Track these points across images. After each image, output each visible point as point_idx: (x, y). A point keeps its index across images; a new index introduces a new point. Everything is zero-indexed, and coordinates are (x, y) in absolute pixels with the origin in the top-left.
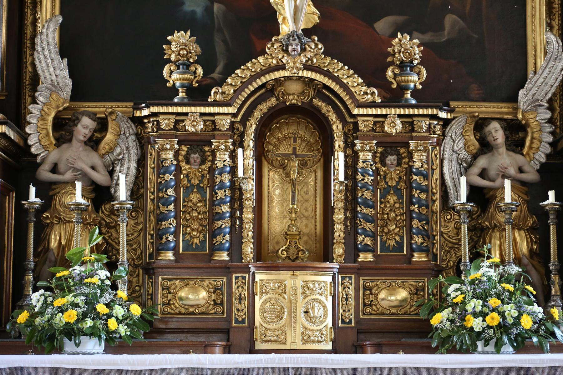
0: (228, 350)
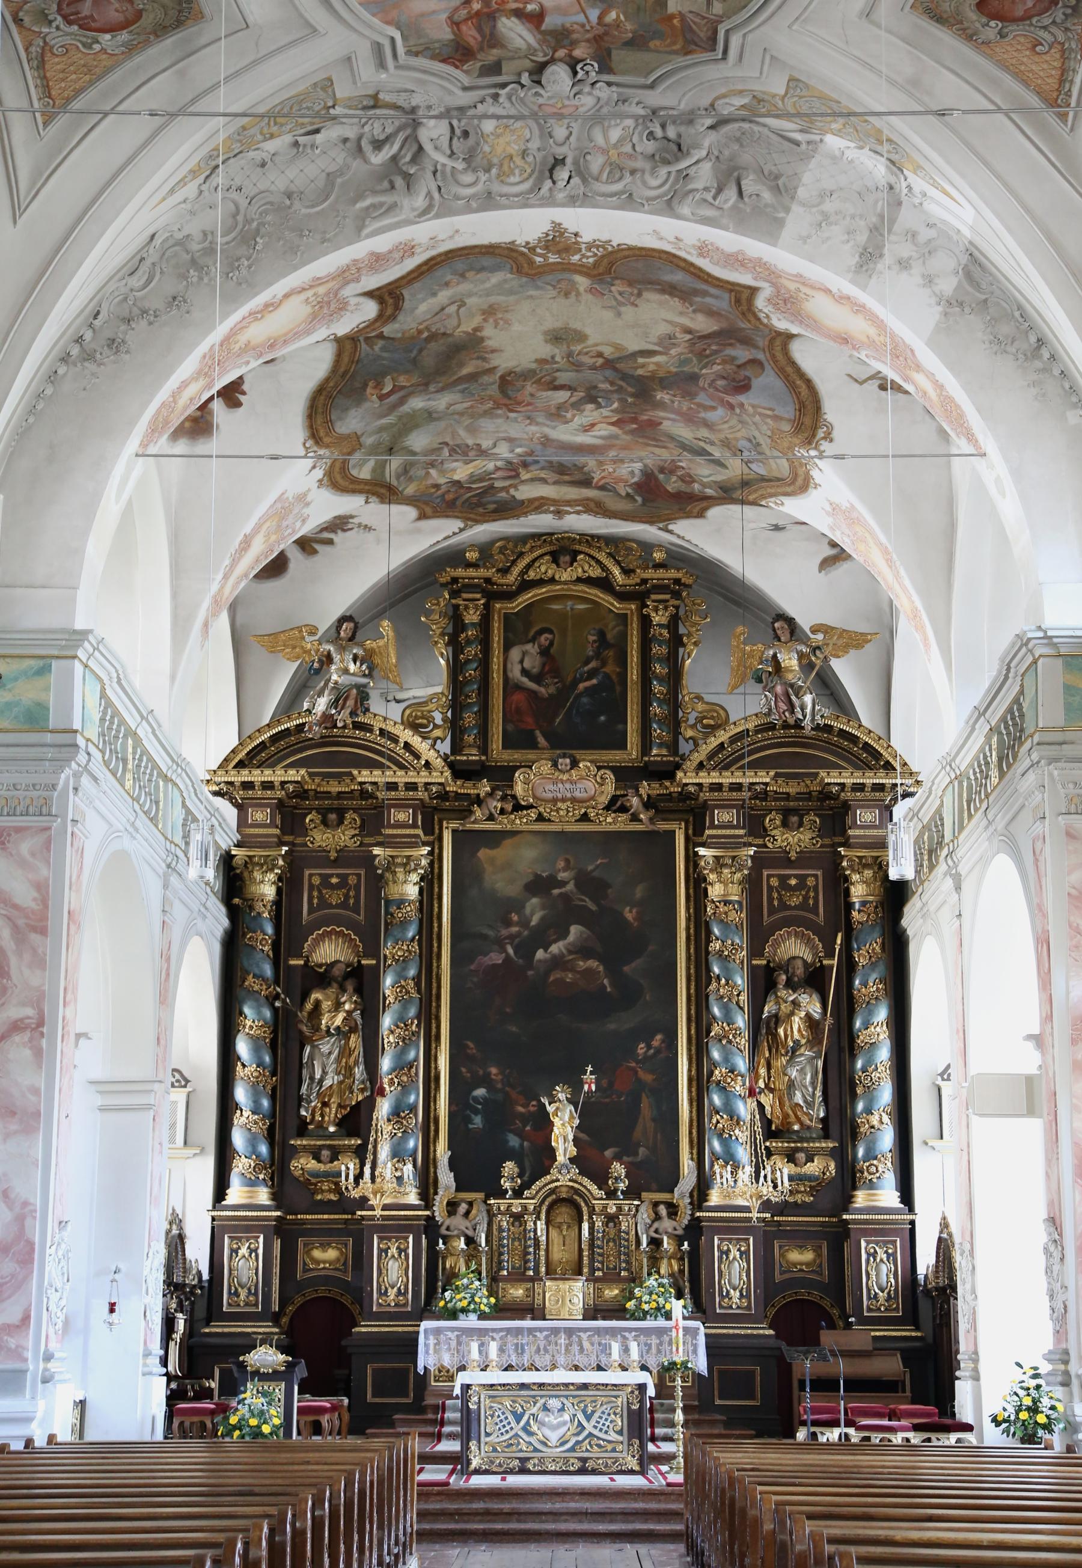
0: (533, 1319)
